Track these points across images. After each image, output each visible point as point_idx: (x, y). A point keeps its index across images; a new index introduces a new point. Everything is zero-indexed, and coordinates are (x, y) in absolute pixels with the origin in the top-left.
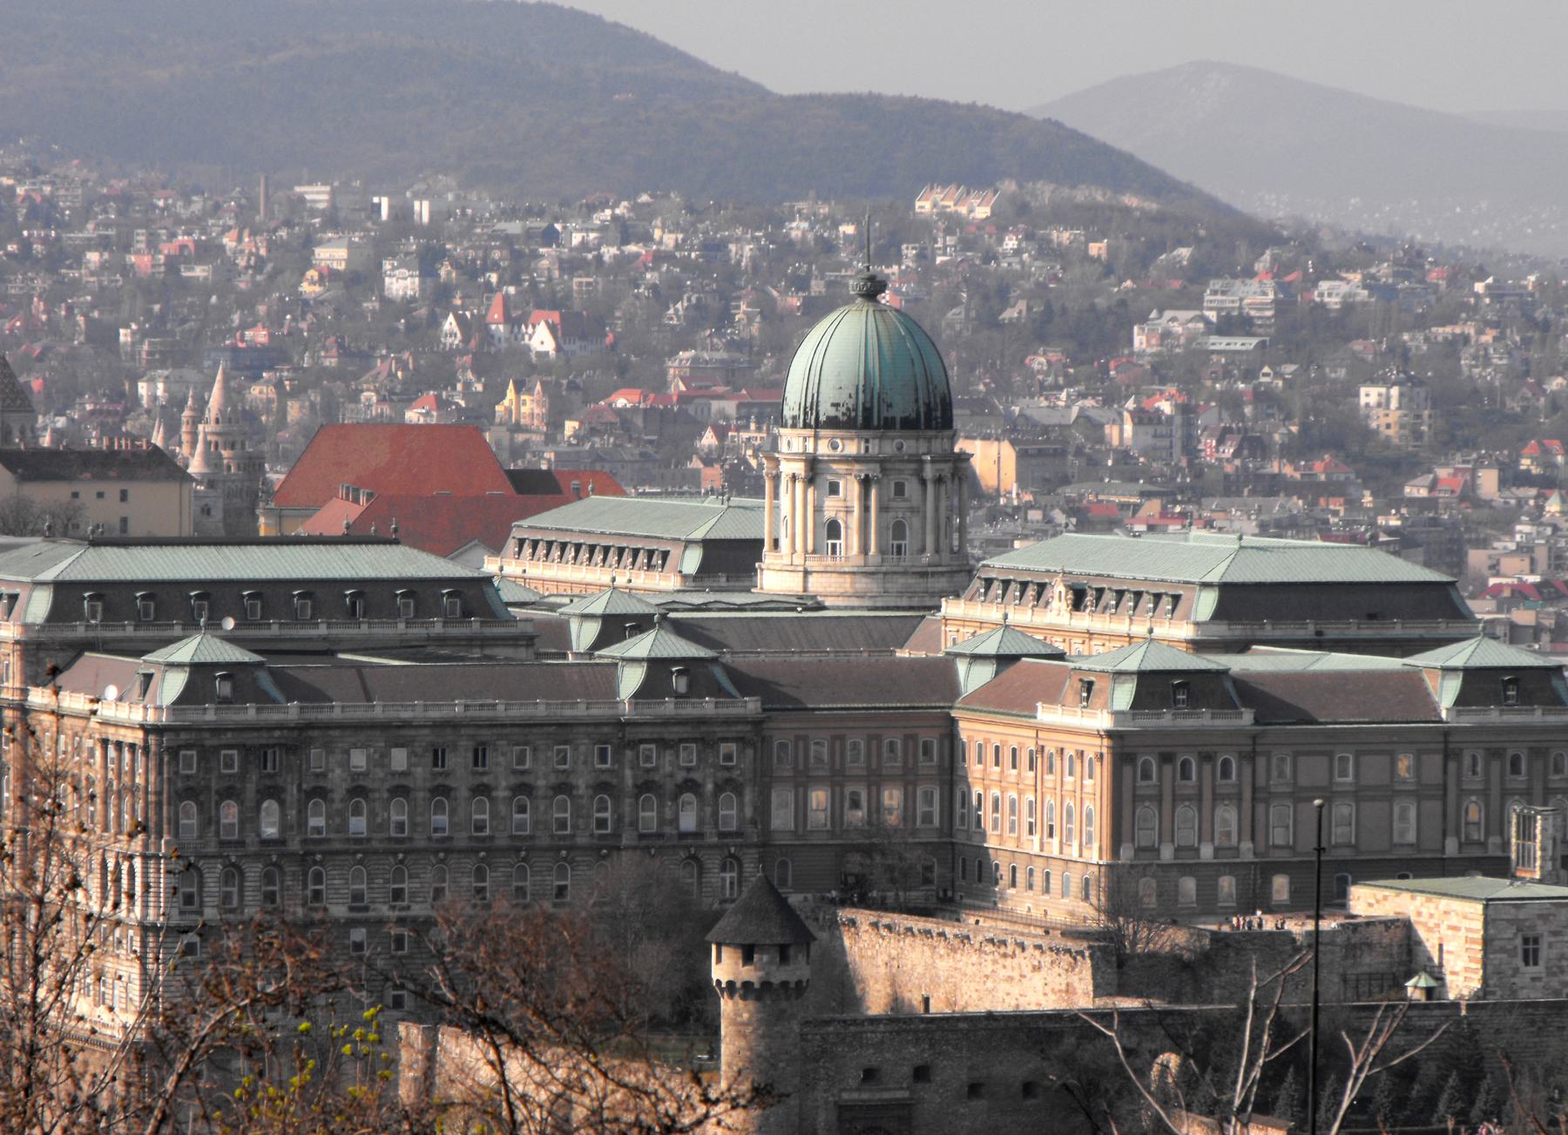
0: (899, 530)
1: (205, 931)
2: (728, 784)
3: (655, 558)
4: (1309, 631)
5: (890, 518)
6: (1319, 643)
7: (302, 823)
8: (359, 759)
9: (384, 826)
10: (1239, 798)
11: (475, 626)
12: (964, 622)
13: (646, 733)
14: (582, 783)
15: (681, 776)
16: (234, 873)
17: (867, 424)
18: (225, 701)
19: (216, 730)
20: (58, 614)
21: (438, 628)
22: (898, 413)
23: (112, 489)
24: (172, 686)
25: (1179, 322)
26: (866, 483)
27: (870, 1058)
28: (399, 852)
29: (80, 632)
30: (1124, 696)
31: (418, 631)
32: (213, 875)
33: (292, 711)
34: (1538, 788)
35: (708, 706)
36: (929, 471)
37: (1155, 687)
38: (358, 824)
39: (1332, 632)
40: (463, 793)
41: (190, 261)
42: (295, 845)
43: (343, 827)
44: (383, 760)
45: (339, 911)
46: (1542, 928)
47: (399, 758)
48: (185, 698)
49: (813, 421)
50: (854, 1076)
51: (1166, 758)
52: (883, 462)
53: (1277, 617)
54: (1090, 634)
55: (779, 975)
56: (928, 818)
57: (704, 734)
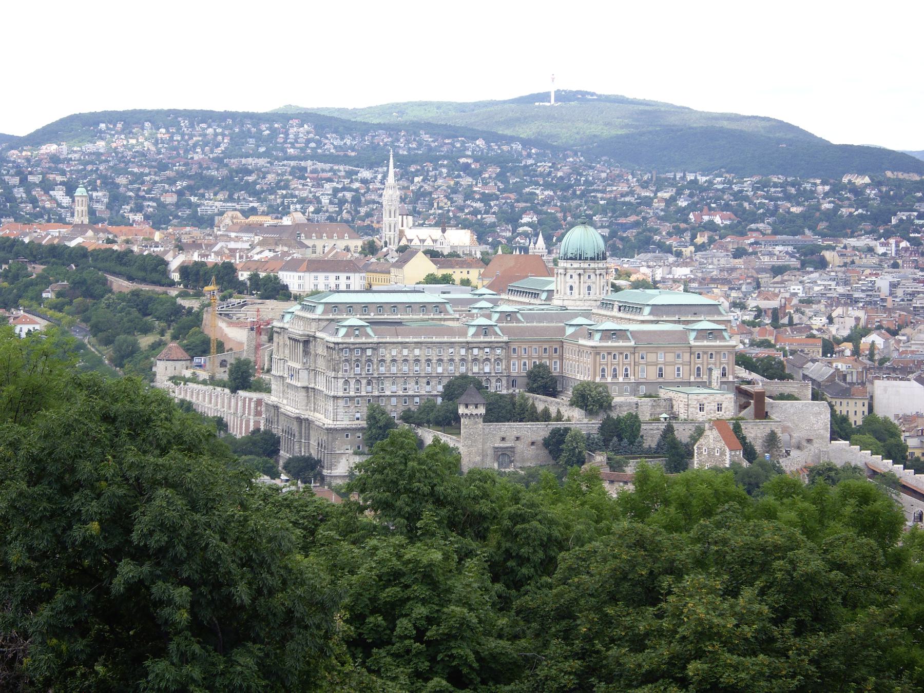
0: (589, 288)
1: (351, 398)
2: (498, 360)
3: (536, 295)
4: (676, 318)
5: (587, 285)
6: (679, 322)
7: (378, 369)
8: (394, 353)
9: (401, 370)
10: (630, 365)
11: (442, 316)
12: (597, 314)
13: (475, 345)
14: (457, 359)
15: (485, 357)
16: (358, 381)
17: (580, 259)
18: (357, 336)
19: (353, 344)
20: (325, 312)
21: (432, 316)
22: (589, 256)
23: (465, 271)
24: (343, 331)
25: (903, 216)
26: (580, 275)
27: (502, 434)
28: (405, 378)
29: (331, 316)
30: (597, 336)
31: (427, 317)
32: (352, 382)
33: (375, 340)
34: (718, 363)
35: (493, 339)
36: (598, 272)
37: (609, 334)
38: (394, 369)
39: (683, 319)
40: (423, 361)
41: (623, 195)
42: (375, 375)
43: (390, 370)
44: (401, 352)
45: (388, 393)
46: (705, 401)
47: (405, 352)
48: (347, 335)
49: (566, 258)
50: (498, 439)
51: (609, 354)
52: (584, 269)
53: (667, 314)
54: (621, 318)
55: (475, 412)
56: (555, 369)
57: (492, 346)
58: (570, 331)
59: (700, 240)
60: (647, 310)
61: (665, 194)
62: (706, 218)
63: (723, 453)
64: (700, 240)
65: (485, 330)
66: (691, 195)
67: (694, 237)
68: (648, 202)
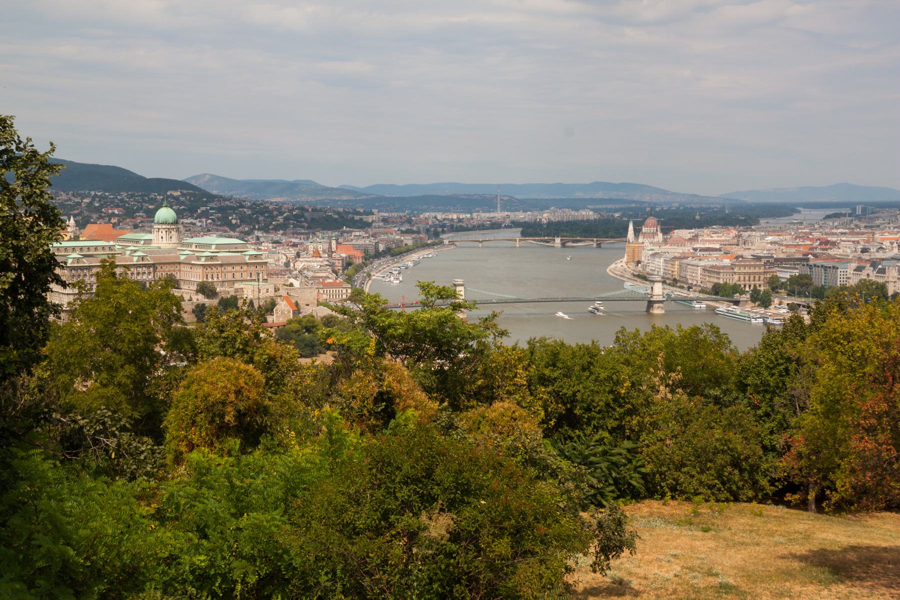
2: (149, 273)
22: (171, 221)
25: (204, 208)
30: (203, 259)
57: (145, 265)
58: (182, 258)
59: (113, 221)
60: (214, 247)
61: (87, 200)
62: (110, 211)
63: (289, 312)
64: (113, 221)
65: (143, 258)
66: (100, 201)
67: (110, 219)
68: (79, 204)
